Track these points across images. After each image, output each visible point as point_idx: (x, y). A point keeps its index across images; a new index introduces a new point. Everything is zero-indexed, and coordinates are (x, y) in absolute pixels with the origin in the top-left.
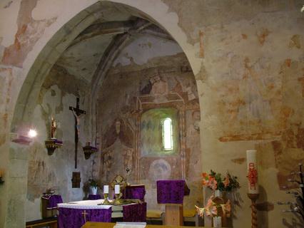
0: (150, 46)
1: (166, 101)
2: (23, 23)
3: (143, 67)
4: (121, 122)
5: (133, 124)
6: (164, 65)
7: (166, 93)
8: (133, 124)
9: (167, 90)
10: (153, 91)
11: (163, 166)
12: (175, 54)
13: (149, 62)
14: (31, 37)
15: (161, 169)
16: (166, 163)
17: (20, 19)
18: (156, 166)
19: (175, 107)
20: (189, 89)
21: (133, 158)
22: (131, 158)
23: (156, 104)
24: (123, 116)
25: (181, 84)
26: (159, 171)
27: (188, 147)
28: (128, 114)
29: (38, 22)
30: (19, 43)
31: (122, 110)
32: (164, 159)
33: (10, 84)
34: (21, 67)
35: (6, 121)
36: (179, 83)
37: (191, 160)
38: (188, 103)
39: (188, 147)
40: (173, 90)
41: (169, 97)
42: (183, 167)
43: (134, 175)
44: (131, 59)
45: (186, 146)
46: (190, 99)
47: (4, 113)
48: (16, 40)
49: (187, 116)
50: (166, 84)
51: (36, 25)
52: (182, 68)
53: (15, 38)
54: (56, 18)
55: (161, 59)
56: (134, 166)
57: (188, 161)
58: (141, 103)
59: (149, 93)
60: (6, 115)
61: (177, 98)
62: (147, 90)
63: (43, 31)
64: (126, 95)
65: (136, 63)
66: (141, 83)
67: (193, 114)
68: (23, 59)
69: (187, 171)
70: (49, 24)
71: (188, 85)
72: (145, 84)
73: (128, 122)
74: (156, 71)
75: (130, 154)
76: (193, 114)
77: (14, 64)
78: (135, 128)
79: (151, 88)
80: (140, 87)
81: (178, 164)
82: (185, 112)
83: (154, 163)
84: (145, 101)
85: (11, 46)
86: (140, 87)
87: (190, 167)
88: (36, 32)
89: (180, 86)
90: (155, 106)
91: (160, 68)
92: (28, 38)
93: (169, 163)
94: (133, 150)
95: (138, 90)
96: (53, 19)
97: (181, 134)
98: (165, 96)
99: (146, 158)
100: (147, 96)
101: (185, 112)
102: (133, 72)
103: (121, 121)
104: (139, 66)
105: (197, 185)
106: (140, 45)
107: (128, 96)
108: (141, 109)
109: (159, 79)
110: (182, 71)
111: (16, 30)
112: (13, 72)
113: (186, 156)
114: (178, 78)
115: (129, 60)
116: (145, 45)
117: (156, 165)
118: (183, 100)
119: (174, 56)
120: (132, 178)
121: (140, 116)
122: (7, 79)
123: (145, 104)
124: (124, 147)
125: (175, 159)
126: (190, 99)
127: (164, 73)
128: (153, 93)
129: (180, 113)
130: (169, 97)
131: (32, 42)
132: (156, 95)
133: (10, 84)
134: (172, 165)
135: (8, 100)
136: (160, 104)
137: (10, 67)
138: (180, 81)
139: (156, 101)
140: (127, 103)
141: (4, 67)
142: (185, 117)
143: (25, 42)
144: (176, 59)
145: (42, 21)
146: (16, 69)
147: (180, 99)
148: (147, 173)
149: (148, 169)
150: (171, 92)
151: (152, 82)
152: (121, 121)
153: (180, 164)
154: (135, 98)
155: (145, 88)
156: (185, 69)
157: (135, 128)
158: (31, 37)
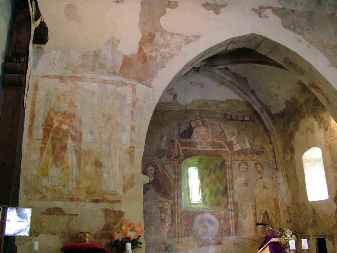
0: (202, 86)
1: (210, 149)
2: (149, 30)
3: (183, 108)
4: (155, 168)
5: (171, 171)
6: (207, 109)
7: (209, 140)
8: (171, 171)
9: (211, 137)
10: (194, 135)
11: (210, 221)
12: (224, 100)
13: (193, 103)
14: (162, 50)
15: (207, 224)
16: (213, 218)
17: (143, 24)
18: (202, 221)
19: (221, 157)
20: (234, 139)
21: (172, 212)
22: (169, 212)
23: (199, 151)
24: (157, 161)
25: (226, 132)
26: (205, 227)
27: (236, 200)
28: (164, 159)
29: (172, 35)
30: (144, 55)
31: (157, 154)
32: (210, 213)
33: (134, 106)
34: (150, 86)
35: (132, 157)
36: (222, 132)
37: (239, 214)
38: (233, 153)
39: (236, 200)
40: (217, 138)
41: (213, 144)
42: (232, 222)
43: (175, 232)
44: (175, 96)
45: (233, 199)
46: (235, 149)
47: (129, 144)
48: (140, 49)
49: (234, 166)
50: (210, 130)
51: (168, 37)
52: (225, 115)
53: (138, 46)
54: (198, 37)
55: (206, 103)
56: (173, 221)
57: (237, 216)
58: (181, 148)
59: (189, 136)
60: (132, 147)
61: (222, 147)
62: (188, 133)
63: (179, 48)
64: (162, 137)
65: (178, 101)
66: (179, 125)
67: (239, 165)
68: (153, 77)
69: (236, 226)
70: (188, 41)
71: (233, 135)
72: (184, 127)
73: (164, 168)
74: (197, 114)
75: (167, 206)
76: (239, 165)
77: (140, 80)
78: (173, 177)
79: (192, 133)
80: (179, 129)
81: (226, 220)
82: (231, 162)
83: (199, 218)
84: (186, 145)
85: (132, 55)
86: (179, 129)
87: (239, 222)
88: (169, 46)
89: (225, 135)
90: (198, 153)
91: (201, 112)
92: (157, 50)
93: (216, 217)
94: (171, 202)
95: (176, 132)
96: (194, 36)
97: (228, 185)
98: (209, 143)
99: (188, 212)
100: (188, 140)
101: (231, 162)
102: (171, 111)
103: (156, 167)
104: (180, 105)
105: (246, 242)
106: (191, 83)
107: (165, 138)
108: (181, 154)
109: (201, 123)
110: (225, 117)
111: (138, 36)
112: (137, 90)
113: (234, 210)
114: (223, 127)
115: (172, 97)
116: (197, 84)
117: (200, 220)
118: (228, 149)
119: (222, 102)
120: (172, 235)
121: (180, 162)
122: (129, 99)
123: (186, 150)
124: (160, 198)
125: (222, 213)
126: (235, 149)
127: (207, 117)
128: (195, 138)
129: (227, 163)
130: (213, 144)
131: (163, 57)
132: (198, 140)
133: (134, 106)
134: (219, 219)
135: (133, 128)
136: (204, 152)
137: (133, 82)
138: (224, 129)
139: (199, 148)
140: (163, 146)
141: (125, 80)
142: (231, 168)
143: (154, 54)
144: (222, 105)
145: (177, 34)
146: (140, 87)
147: (225, 148)
148: (191, 230)
149: (192, 225)
150: (215, 140)
151: (193, 125)
152: (156, 167)
153: (229, 218)
154: (173, 141)
155: (185, 131)
156: (230, 118)
157: (173, 177)
158: (162, 50)
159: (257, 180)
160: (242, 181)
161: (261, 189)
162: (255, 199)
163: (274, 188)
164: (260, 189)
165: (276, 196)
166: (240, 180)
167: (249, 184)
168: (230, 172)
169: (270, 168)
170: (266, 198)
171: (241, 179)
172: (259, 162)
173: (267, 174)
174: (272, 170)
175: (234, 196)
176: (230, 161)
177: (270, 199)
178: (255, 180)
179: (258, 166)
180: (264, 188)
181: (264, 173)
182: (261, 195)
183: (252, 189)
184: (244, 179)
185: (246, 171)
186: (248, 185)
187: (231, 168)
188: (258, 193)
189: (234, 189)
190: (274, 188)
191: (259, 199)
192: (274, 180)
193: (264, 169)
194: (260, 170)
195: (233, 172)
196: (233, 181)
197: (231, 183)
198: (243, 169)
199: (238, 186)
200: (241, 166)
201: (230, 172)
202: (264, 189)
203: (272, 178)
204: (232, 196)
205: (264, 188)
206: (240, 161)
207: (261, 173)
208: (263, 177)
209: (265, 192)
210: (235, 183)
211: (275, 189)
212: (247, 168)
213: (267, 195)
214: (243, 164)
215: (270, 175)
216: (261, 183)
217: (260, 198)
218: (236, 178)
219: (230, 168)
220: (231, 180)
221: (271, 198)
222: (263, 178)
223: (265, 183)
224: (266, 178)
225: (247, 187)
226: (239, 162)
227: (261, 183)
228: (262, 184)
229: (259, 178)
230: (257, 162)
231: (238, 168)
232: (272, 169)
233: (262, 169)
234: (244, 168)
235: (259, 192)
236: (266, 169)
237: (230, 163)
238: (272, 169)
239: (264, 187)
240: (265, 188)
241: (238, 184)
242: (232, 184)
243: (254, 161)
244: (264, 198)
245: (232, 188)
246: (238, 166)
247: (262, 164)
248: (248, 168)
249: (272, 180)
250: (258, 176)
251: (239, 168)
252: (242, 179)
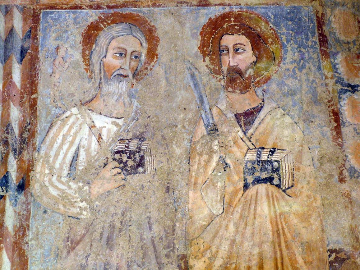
159: (213, 130)
160: (100, 137)
161: (235, 193)
162: (184, 258)
163: (342, 180)
164: (230, 189)
165: (349, 240)
166: (86, 129)
167: (147, 158)
168: (17, 77)
169: (326, 55)
170: (268, 249)
171: (92, 126)
172: (238, 17)
173: (292, 93)
174: (342, 69)
175: (30, 234)
176: (23, 10)
177: (300, 261)
178: (202, 130)
179: (229, 40)
180: (258, 181)
181: (273, 86)
182: (232, 227)
183: (168, 189)
184: (120, 122)
185: (135, 75)
186: (141, 164)
187: (28, 57)
188: (212, 218)
189: (35, 187)
190: (342, 180)
191: (213, 257)
192: (345, 130)
193: (272, 58)
194: (242, 67)
195: (42, 80)
196: (33, 135)
197: (18, 152)
198: (111, 60)
199: (66, 172)
200: (102, 39)
201: (17, 77)
202: (262, 188)
203: (336, 115)
204: (10, 240)
205: (265, 181)
206: (98, 7)
207: (246, 88)
208: (259, 109)
209: (264, 208)
210: (42, 152)
211: (345, 187)
212: (144, 52)
213: (277, 233)
214: (116, 29)
215: (316, 101)
216: (238, 153)
217: (225, 247)
218: (58, 117)
219: (23, 52)
220: (17, 131)
221: (308, 247)
222: (262, 114)
223: (273, 152)
224: (288, 119)
225: (135, 180)
226: (92, 16)
227: (238, 153)
228: (252, 156)
229: (230, 116)
230: (224, 17)
231: (77, 56)
232: (339, 58)
233: (259, 59)
234: (122, 54)
235: (217, 209)
236: (289, 57)
237: (25, 20)
238: (339, 58)
239: (264, 175)
240: (270, 180)
241: (73, 150)
242: (26, 156)
243: (203, 11)
244: (256, 251)
245: (22, 187)
246: (79, 39)
247: (262, 28)
248: (152, 54)
249: (328, 131)
250: (223, 106)
251: (87, 56)
252: (100, 121)
